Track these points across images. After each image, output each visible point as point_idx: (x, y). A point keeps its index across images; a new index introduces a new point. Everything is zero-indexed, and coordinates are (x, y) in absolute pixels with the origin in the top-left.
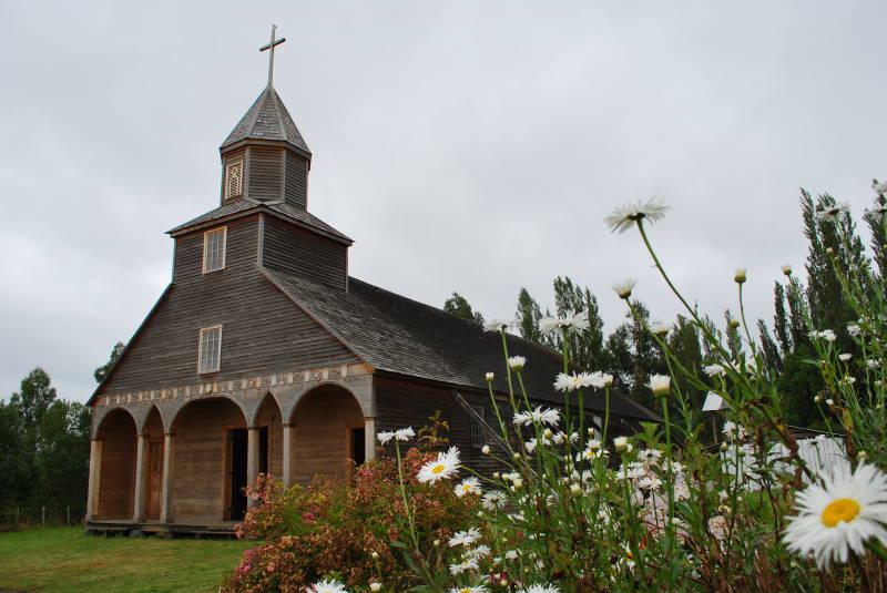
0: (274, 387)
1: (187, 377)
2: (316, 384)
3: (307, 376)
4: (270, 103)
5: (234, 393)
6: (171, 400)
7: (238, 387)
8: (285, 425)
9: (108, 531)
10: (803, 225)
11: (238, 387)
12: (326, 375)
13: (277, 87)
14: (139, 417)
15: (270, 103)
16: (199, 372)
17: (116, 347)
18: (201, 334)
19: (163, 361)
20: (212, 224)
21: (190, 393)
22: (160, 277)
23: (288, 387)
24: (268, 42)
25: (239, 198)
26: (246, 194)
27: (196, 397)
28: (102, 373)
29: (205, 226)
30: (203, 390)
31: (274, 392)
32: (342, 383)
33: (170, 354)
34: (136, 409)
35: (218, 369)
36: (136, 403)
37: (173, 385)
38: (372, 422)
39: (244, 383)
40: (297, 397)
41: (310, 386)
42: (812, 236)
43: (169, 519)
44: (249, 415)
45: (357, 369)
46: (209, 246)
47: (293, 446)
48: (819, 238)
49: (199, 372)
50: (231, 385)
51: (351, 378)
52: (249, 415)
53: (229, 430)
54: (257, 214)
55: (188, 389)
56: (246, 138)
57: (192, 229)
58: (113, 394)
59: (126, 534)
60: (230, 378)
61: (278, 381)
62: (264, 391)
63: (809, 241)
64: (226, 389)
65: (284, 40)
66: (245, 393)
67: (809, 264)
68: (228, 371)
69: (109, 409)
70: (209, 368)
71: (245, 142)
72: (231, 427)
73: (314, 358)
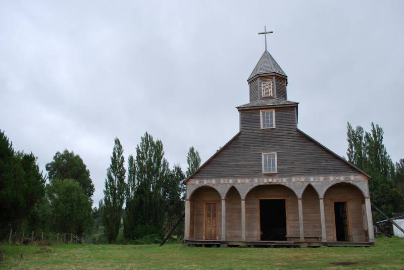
0: (312, 182)
1: (257, 173)
2: (337, 182)
3: (331, 178)
4: (267, 56)
5: (287, 183)
6: (245, 185)
7: (290, 181)
8: (243, 200)
9: (205, 245)
10: (347, 137)
11: (290, 181)
12: (342, 179)
13: (268, 50)
14: (223, 190)
15: (267, 56)
16: (264, 172)
17: (57, 154)
18: (263, 155)
19: (239, 166)
20: (266, 107)
21: (257, 182)
22: (232, 127)
23: (322, 183)
24: (264, 31)
25: (271, 98)
26: (276, 96)
27: (262, 184)
28: (50, 166)
29: (262, 107)
30: (265, 181)
31: (313, 184)
32: (351, 182)
33: (242, 163)
34: (219, 187)
35: (276, 172)
36: (222, 186)
37: (245, 177)
38: (369, 199)
39: (294, 179)
40: (326, 188)
41: (333, 183)
42: (349, 141)
43: (247, 238)
44: (299, 193)
45: (359, 177)
46: (264, 118)
47: (325, 205)
48: (353, 143)
49: (264, 172)
50: (285, 180)
51: (356, 181)
52: (299, 193)
53: (261, 201)
54: (294, 106)
55: (256, 180)
56: (275, 73)
57: (252, 108)
58: (202, 178)
59: (218, 246)
60: (285, 176)
61: (315, 179)
62: (306, 184)
63: (349, 143)
64: (284, 181)
65: (272, 32)
66: (297, 184)
67: (348, 152)
68: (281, 173)
69: (198, 186)
70: (269, 171)
71: (273, 74)
72: (261, 199)
73: (336, 171)
